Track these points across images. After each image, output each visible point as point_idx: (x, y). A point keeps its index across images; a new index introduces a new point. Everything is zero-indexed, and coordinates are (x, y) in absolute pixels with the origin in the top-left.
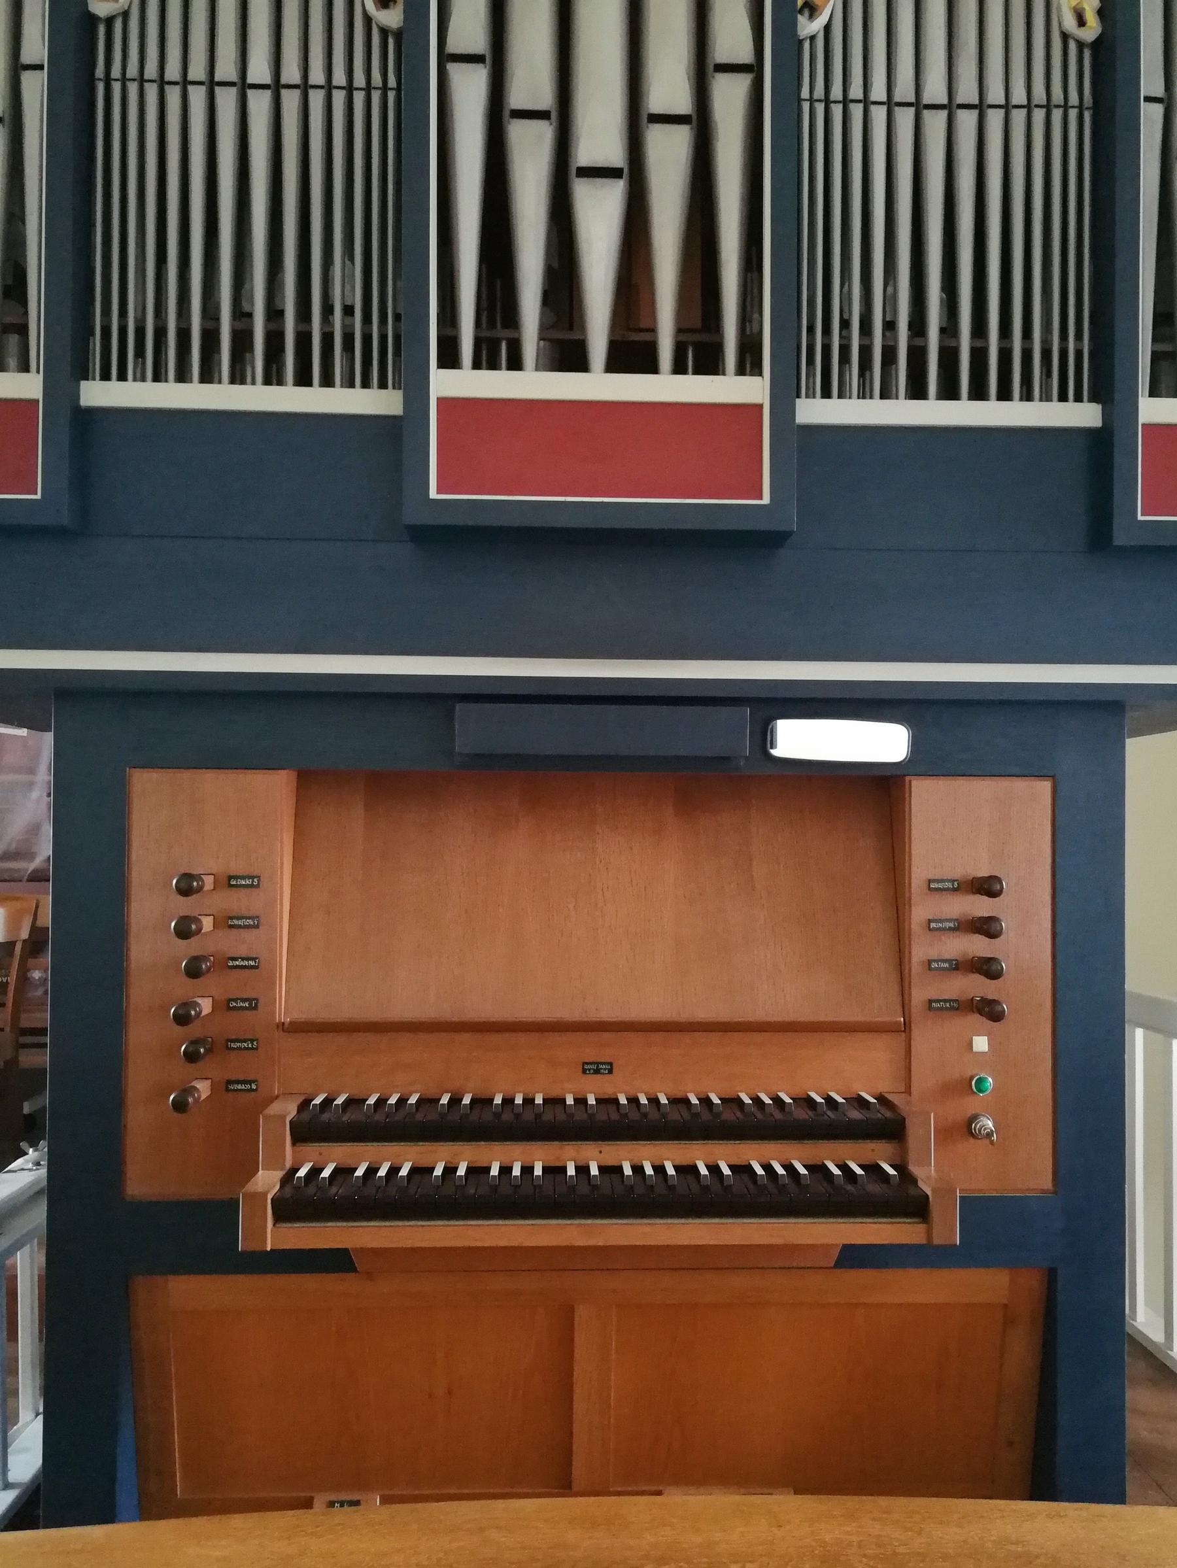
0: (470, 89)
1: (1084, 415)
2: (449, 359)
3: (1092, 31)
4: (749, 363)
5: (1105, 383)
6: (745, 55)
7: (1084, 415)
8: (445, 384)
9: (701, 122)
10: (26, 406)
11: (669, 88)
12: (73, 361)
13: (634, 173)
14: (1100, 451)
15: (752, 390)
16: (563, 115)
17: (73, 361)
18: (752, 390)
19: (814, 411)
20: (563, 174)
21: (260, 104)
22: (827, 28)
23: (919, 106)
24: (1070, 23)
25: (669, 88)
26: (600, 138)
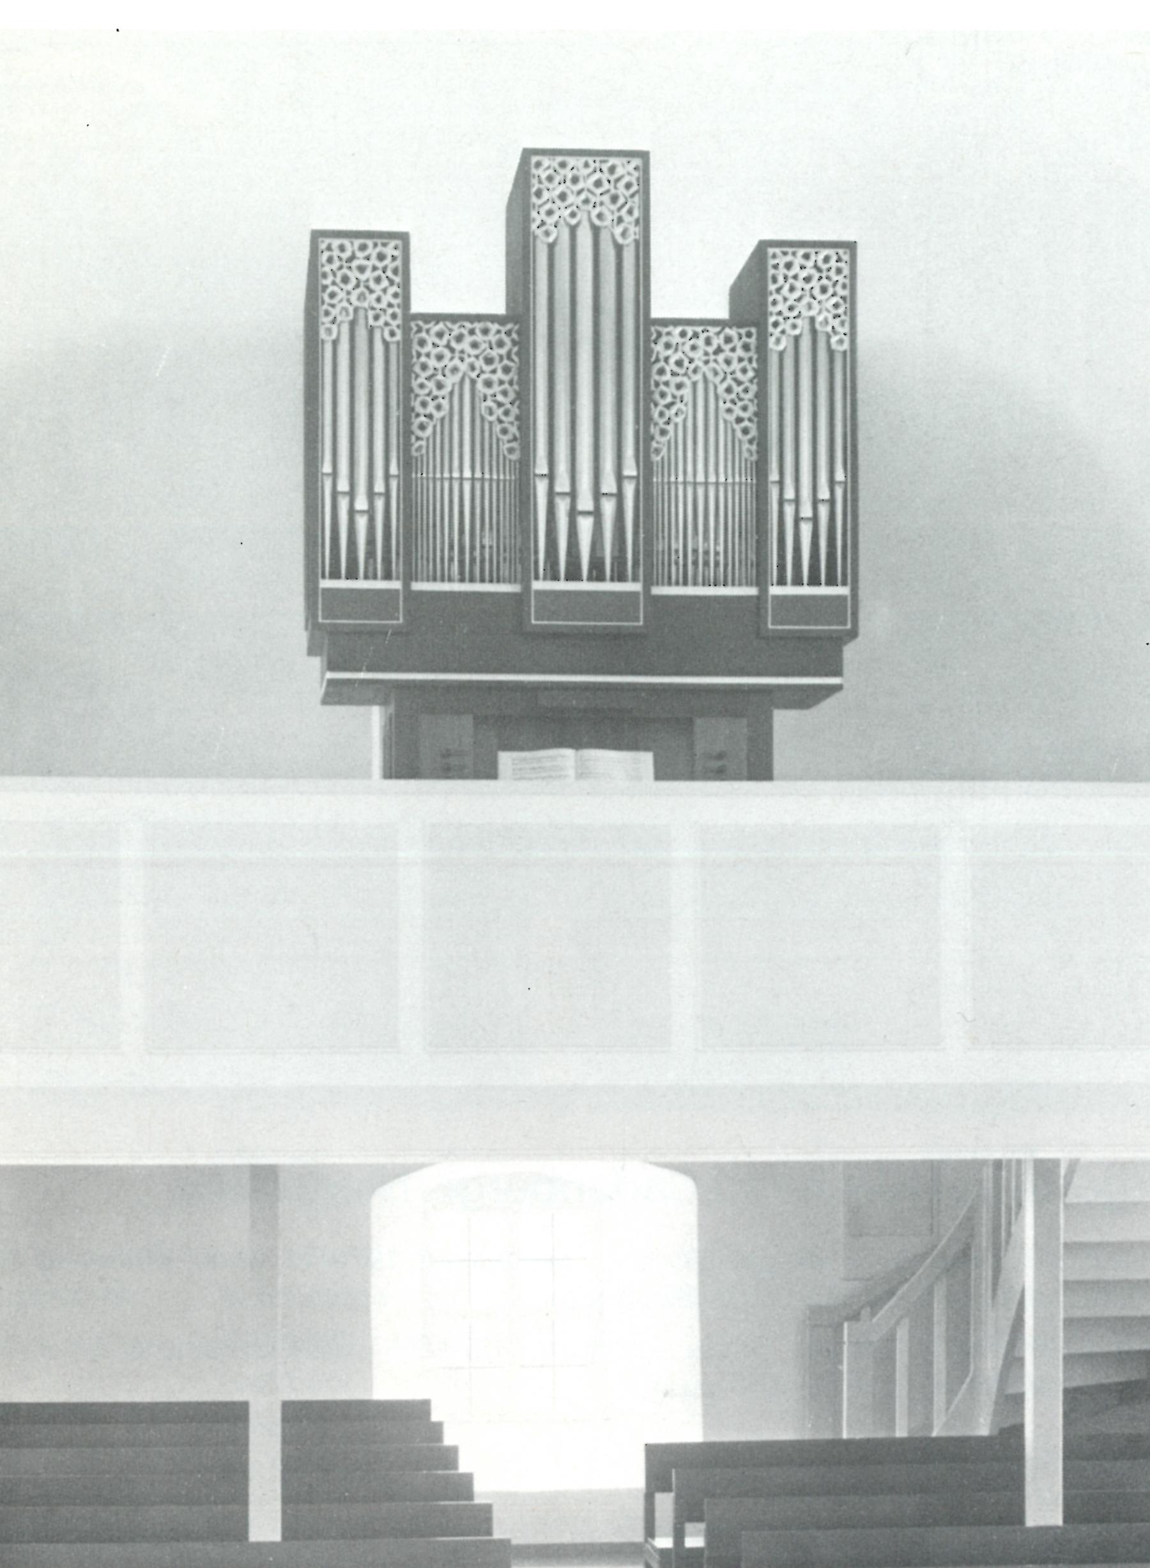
0: (542, 487)
1: (752, 591)
2: (537, 578)
3: (754, 458)
4: (635, 579)
5: (761, 581)
6: (634, 473)
7: (752, 591)
8: (538, 585)
9: (620, 496)
10: (397, 591)
11: (609, 485)
12: (408, 578)
13: (597, 513)
14: (759, 601)
15: (635, 587)
16: (573, 495)
17: (408, 578)
18: (635, 587)
19: (657, 591)
20: (573, 514)
21: (467, 487)
22: (663, 458)
23: (695, 484)
24: (745, 455)
25: (609, 485)
26: (585, 502)
